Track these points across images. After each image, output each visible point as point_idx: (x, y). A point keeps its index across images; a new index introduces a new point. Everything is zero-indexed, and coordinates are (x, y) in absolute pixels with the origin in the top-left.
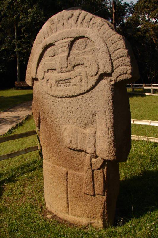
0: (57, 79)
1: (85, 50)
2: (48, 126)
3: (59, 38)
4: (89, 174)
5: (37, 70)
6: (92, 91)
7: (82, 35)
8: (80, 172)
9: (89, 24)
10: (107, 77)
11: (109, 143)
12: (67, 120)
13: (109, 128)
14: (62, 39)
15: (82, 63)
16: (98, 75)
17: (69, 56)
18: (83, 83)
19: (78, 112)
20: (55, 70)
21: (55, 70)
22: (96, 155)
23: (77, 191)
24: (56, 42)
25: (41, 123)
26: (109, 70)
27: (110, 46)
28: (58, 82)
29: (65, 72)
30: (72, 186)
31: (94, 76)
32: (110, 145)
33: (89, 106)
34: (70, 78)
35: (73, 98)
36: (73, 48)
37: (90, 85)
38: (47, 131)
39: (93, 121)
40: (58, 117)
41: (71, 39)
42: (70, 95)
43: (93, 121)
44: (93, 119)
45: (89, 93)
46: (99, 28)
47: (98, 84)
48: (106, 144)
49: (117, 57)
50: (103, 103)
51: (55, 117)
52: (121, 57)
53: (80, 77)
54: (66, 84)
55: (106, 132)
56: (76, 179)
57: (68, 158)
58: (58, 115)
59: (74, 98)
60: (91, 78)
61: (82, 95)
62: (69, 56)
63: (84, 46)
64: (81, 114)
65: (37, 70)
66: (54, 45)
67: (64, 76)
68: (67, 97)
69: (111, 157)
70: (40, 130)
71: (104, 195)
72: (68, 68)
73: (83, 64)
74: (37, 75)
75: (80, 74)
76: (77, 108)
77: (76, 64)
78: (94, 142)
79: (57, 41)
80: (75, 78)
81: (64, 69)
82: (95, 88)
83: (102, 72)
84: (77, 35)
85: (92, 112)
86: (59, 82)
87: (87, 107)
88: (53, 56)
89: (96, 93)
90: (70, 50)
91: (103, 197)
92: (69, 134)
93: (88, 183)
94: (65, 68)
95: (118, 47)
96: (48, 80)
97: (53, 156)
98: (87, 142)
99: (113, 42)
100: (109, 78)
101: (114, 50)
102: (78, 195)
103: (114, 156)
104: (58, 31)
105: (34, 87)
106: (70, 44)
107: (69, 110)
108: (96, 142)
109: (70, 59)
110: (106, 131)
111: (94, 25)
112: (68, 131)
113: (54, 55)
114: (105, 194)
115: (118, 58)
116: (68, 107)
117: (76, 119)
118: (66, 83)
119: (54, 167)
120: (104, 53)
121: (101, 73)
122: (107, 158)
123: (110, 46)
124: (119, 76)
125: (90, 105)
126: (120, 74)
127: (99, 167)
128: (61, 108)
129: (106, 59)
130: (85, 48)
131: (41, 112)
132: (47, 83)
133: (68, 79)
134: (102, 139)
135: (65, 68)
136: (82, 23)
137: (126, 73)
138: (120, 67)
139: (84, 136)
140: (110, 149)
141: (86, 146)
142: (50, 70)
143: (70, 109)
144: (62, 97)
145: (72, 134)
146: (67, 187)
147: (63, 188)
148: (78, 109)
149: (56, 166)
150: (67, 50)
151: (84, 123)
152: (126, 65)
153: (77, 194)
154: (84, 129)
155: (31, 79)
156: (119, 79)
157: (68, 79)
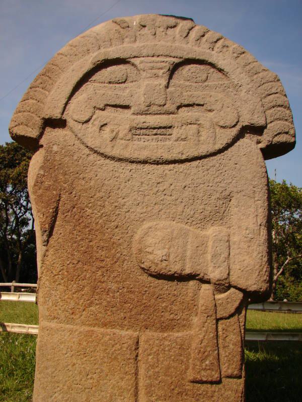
0: (135, 125)
1: (206, 83)
2: (86, 227)
3: (145, 52)
4: (210, 330)
5: (66, 104)
6: (222, 154)
7: (201, 58)
8: (178, 331)
9: (214, 46)
10: (252, 136)
11: (261, 255)
12: (155, 211)
13: (260, 225)
14: (153, 56)
15: (202, 103)
16: (238, 127)
17: (167, 87)
18: (202, 138)
19: (187, 193)
20: (127, 107)
21: (127, 107)
22: (229, 283)
23: (170, 381)
24: (135, 57)
25: (57, 223)
26: (261, 122)
27: (259, 86)
28: (137, 130)
29: (157, 114)
30: (157, 370)
32: (262, 259)
33: (215, 181)
34: (170, 125)
35: (171, 166)
36: (176, 76)
37: (221, 142)
38: (82, 239)
39: (224, 213)
40: (127, 204)
41: (177, 61)
42: (167, 156)
43: (224, 213)
44: (224, 208)
45: (215, 157)
46: (235, 55)
47: (236, 144)
48: (254, 257)
49: (272, 104)
50: (249, 176)
51: (116, 204)
52: (279, 106)
53: (195, 126)
54: (156, 136)
55: (255, 232)
56: (169, 350)
57: (144, 301)
58: (124, 200)
59: (176, 165)
60: (222, 130)
61: (199, 161)
62: (167, 87)
63: (204, 77)
64: (194, 199)
65: (66, 104)
66: (128, 62)
67: (152, 120)
68: (157, 163)
69: (263, 284)
70: (52, 241)
71: (240, 377)
72: (165, 106)
73: (203, 105)
74: (65, 113)
75: (196, 120)
76: (184, 184)
77: (186, 102)
78: (227, 254)
79: (137, 57)
80: (184, 127)
81: (154, 108)
82: (229, 150)
83: (246, 124)
84: (190, 56)
85: (223, 194)
86: (138, 132)
87: (211, 185)
88: (122, 83)
89: (232, 159)
90: (170, 78)
91: (239, 381)
92: (162, 240)
93: (206, 353)
94: (160, 106)
95: (274, 91)
96: (106, 124)
97: (90, 304)
98: (209, 257)
99: (264, 81)
100: (256, 138)
101: (267, 93)
102: (173, 389)
103: (267, 283)
104: (138, 41)
105: (42, 142)
106: (171, 67)
107: (161, 189)
108: (231, 254)
109: (171, 93)
110: (255, 230)
111: (225, 49)
112: (159, 233)
113: (124, 82)
114: (243, 374)
115: (273, 107)
116: (159, 183)
117: (180, 209)
118: (156, 134)
119: (90, 334)
120: (251, 93)
121: (244, 125)
122: (255, 286)
123: (259, 86)
124: (276, 135)
125: (218, 180)
126: (278, 132)
127: (232, 309)
128: (138, 184)
129: (256, 104)
131: (64, 197)
132: (100, 130)
133: (165, 128)
134: (246, 246)
135: (160, 106)
136: (199, 41)
137: (287, 133)
138: (279, 122)
139: (203, 244)
140: (262, 267)
141: (205, 264)
142: (108, 107)
143: (165, 187)
144: (145, 162)
145: (171, 240)
146: (136, 378)
147: (122, 384)
148: (186, 188)
149: (99, 330)
150: (165, 75)
151: (202, 217)
152: (286, 120)
153: (172, 387)
154: (200, 229)
155: (39, 122)
156: (277, 139)
157: (165, 128)
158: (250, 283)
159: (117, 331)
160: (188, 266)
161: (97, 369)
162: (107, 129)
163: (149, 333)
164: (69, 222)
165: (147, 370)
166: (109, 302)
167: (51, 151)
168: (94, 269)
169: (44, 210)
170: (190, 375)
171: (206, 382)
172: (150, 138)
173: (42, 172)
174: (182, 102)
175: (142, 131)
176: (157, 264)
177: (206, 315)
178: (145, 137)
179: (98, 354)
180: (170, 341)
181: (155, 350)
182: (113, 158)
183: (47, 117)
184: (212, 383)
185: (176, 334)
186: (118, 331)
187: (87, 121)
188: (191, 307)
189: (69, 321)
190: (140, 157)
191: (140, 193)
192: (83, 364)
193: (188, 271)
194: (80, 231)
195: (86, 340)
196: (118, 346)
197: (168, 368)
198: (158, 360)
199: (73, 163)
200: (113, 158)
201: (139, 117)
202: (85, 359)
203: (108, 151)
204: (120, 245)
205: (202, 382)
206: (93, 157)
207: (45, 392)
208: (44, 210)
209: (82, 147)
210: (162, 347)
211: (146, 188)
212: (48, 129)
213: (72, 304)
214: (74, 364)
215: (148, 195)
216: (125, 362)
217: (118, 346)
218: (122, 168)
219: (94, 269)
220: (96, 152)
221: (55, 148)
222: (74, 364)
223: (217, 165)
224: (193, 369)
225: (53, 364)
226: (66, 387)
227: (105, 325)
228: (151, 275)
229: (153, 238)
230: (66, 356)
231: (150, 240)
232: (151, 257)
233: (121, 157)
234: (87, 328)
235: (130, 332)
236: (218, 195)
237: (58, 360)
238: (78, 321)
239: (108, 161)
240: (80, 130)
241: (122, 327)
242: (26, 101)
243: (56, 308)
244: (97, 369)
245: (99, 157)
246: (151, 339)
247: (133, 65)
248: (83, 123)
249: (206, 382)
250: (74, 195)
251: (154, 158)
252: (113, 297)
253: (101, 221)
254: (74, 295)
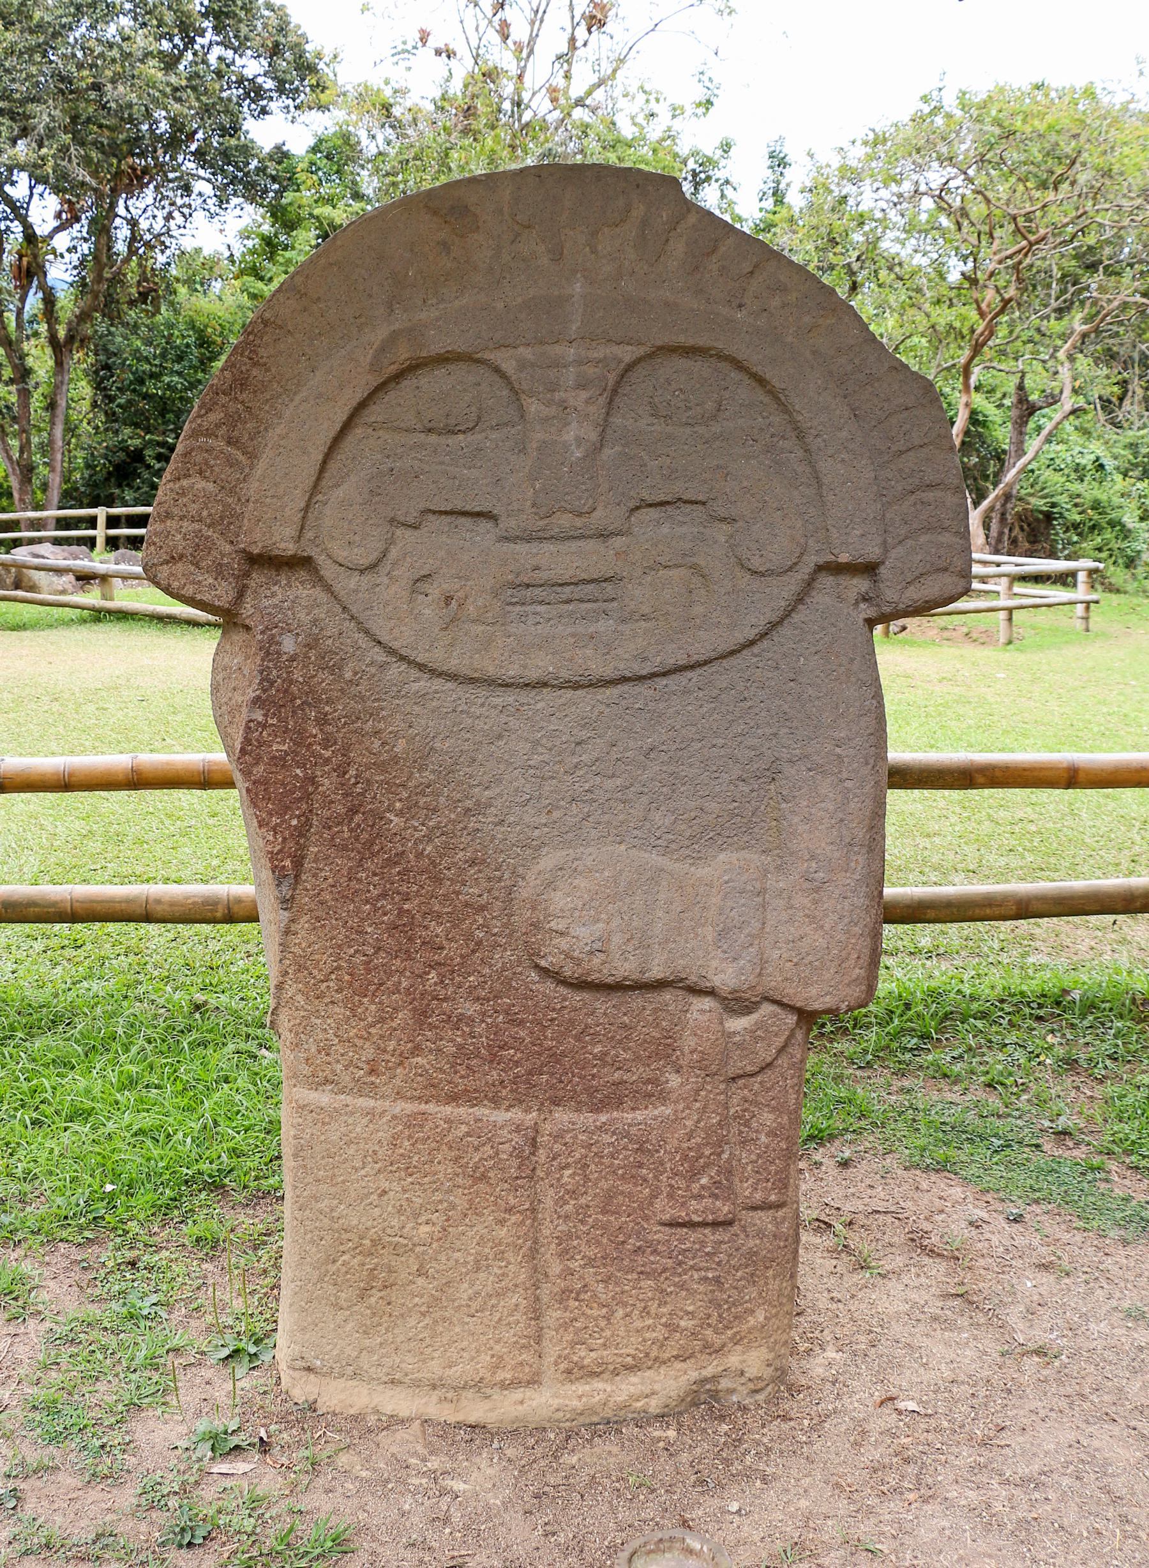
1: (716, 428)
2: (391, 862)
15: (701, 498)
16: (805, 571)
23: (617, 1225)
30: (583, 1201)
31: (780, 574)
38: (383, 895)
40: (498, 803)
41: (627, 354)
51: (469, 803)
54: (571, 607)
63: (710, 405)
97: (417, 1050)
116: (578, 744)
119: (415, 1122)
125: (740, 728)
130: (714, 417)
131: (326, 784)
148: (652, 756)
153: (621, 1238)
158: (813, 991)
159: (478, 1111)
160: (656, 961)
161: (441, 1202)
162: (435, 590)
163: (562, 1116)
164: (345, 848)
165: (561, 1201)
166: (460, 1047)
167: (278, 653)
168: (419, 968)
169: (275, 820)
170: (664, 1209)
171: (704, 1224)
172: (553, 610)
173: (259, 716)
174: (645, 495)
175: (529, 593)
176: (578, 962)
177: (703, 1073)
178: (539, 608)
179: (441, 1168)
180: (614, 1133)
181: (578, 1156)
182: (452, 677)
183: (256, 551)
184: (715, 1224)
185: (629, 1116)
186: (487, 1112)
187: (373, 567)
188: (664, 1049)
189: (361, 1088)
190: (527, 673)
191: (532, 771)
192: (405, 1191)
193: (656, 972)
194: (375, 874)
195: (410, 1137)
196: (488, 1150)
197: (610, 1196)
198: (586, 1178)
199: (342, 690)
200: (452, 677)
201: (521, 548)
202: (410, 1180)
203: (436, 657)
204: (483, 908)
205: (691, 1225)
206: (396, 670)
207: (319, 1251)
208: (275, 820)
209: (363, 641)
210: (594, 1149)
211: (546, 757)
212: (257, 578)
213: (369, 1052)
214: (385, 1192)
215: (553, 778)
216: (506, 1186)
217: (488, 1150)
218: (480, 701)
219: (419, 968)
220: (403, 658)
221: (289, 645)
222: (385, 1192)
223: (741, 686)
224: (670, 1196)
225: (333, 1190)
226: (367, 1242)
227: (453, 1098)
228: (564, 982)
229: (568, 895)
230: (363, 1172)
231: (559, 900)
232: (564, 943)
233: (476, 675)
234: (410, 1107)
235: (516, 1114)
236: (736, 772)
237: (343, 1182)
238: (387, 1090)
239: (438, 684)
240: (356, 591)
241: (496, 1102)
242: (185, 483)
243: (329, 1059)
244: (441, 1202)
245: (414, 673)
246: (567, 1132)
247: (497, 370)
248: (362, 572)
249: (704, 1224)
250: (353, 780)
251: (565, 674)
252: (472, 1035)
253: (429, 849)
254: (373, 1031)
